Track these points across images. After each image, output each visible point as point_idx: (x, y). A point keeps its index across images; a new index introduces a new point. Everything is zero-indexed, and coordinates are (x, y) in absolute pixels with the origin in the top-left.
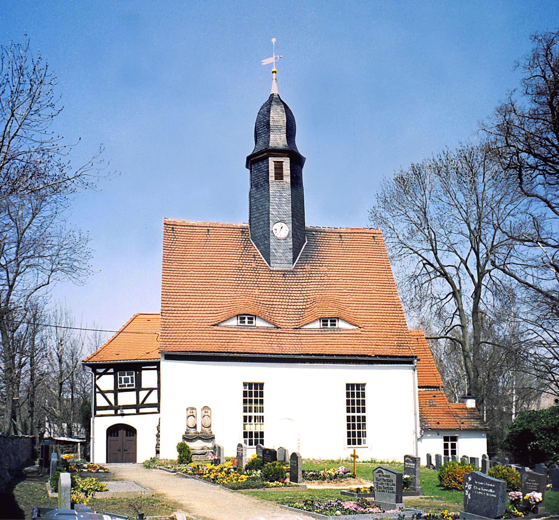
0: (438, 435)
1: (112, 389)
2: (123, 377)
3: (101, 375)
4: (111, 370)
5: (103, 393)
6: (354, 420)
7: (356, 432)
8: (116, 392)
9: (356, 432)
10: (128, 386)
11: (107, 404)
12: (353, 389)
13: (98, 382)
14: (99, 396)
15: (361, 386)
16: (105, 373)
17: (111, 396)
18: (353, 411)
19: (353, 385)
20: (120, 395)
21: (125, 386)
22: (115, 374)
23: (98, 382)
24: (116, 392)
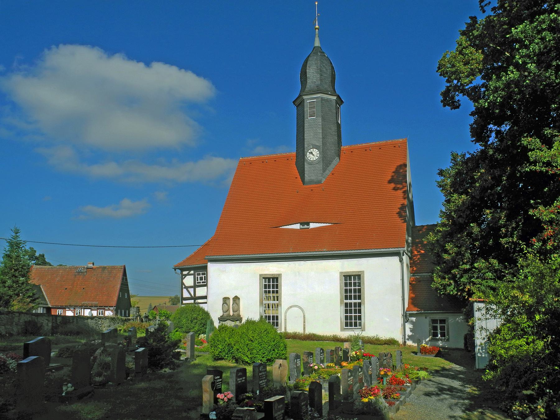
0: (426, 318)
1: (192, 284)
2: (199, 277)
3: (186, 275)
4: (192, 272)
5: (187, 288)
6: (351, 306)
7: (353, 314)
8: (195, 287)
9: (353, 314)
10: (203, 282)
11: (189, 296)
12: (350, 279)
13: (184, 281)
14: (185, 290)
15: (358, 276)
16: (188, 274)
17: (192, 290)
18: (351, 299)
19: (350, 276)
20: (198, 289)
21: (200, 283)
22: (194, 275)
23: (184, 281)
24: (195, 287)
